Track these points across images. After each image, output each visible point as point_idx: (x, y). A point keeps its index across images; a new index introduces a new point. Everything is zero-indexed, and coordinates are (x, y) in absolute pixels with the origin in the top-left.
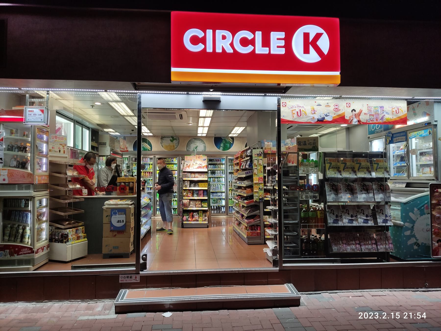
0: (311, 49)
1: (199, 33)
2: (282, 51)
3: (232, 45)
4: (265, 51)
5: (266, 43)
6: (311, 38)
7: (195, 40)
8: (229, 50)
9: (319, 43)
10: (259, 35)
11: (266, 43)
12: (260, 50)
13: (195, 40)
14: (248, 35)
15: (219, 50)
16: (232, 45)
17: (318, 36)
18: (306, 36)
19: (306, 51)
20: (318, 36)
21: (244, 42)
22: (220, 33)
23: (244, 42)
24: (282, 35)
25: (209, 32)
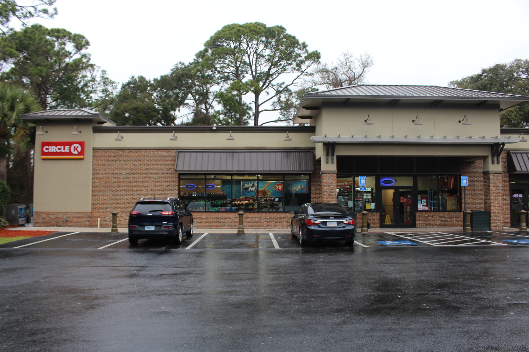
0: (76, 150)
1: (47, 147)
2: (68, 151)
3: (55, 150)
4: (64, 151)
5: (64, 149)
6: (76, 147)
7: (47, 149)
8: (55, 151)
9: (78, 149)
10: (62, 147)
11: (64, 149)
12: (63, 151)
13: (47, 149)
14: (60, 147)
15: (52, 151)
16: (55, 150)
17: (78, 147)
18: (75, 147)
19: (74, 151)
20: (78, 147)
21: (59, 149)
22: (53, 147)
23: (59, 149)
24: (68, 147)
25: (50, 147)
